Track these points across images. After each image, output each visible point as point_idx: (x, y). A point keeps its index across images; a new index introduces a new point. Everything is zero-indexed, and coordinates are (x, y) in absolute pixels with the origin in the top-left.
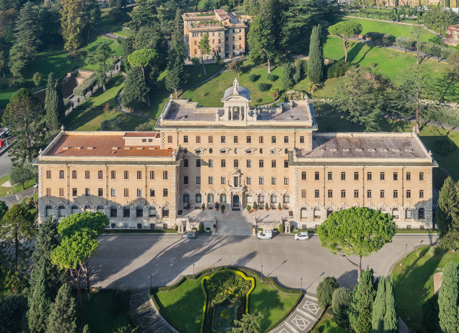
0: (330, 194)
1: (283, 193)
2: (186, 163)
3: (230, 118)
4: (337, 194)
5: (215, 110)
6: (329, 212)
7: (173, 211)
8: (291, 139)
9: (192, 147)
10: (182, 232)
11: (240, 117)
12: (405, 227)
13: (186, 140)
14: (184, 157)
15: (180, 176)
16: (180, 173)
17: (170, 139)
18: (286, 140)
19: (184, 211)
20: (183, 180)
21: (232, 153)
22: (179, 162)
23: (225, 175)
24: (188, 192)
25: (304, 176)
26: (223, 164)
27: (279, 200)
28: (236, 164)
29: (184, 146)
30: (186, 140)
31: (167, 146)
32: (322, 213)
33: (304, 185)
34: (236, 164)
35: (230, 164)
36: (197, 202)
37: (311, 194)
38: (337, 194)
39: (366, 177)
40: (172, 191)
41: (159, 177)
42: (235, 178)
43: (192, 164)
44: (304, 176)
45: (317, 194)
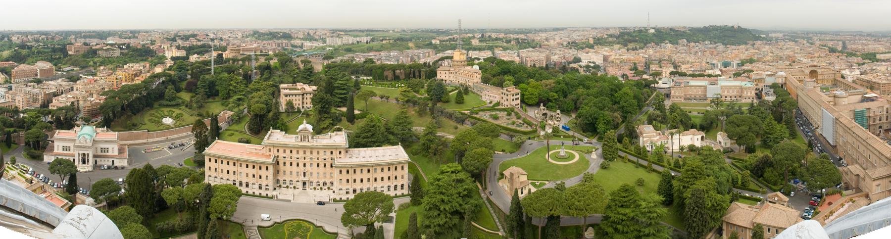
0: (355, 181)
1: (330, 181)
2: (278, 163)
3: (301, 141)
4: (358, 181)
5: (294, 136)
6: (355, 191)
7: (271, 188)
8: (334, 152)
9: (281, 154)
10: (276, 199)
11: (307, 139)
12: (394, 195)
13: (278, 151)
14: (277, 160)
15: (275, 170)
16: (275, 168)
17: (270, 150)
18: (332, 153)
19: (277, 188)
20: (276, 172)
21: (303, 159)
22: (274, 163)
23: (298, 170)
24: (279, 178)
25: (341, 172)
26: (298, 165)
27: (328, 185)
28: (305, 165)
29: (277, 154)
30: (278, 151)
31: (268, 153)
32: (351, 191)
33: (341, 177)
34: (305, 165)
35: (301, 165)
36: (284, 184)
37: (344, 181)
38: (358, 181)
39: (374, 171)
40: (271, 177)
41: (264, 168)
42: (304, 173)
43: (281, 164)
44: (341, 172)
45: (348, 181)
